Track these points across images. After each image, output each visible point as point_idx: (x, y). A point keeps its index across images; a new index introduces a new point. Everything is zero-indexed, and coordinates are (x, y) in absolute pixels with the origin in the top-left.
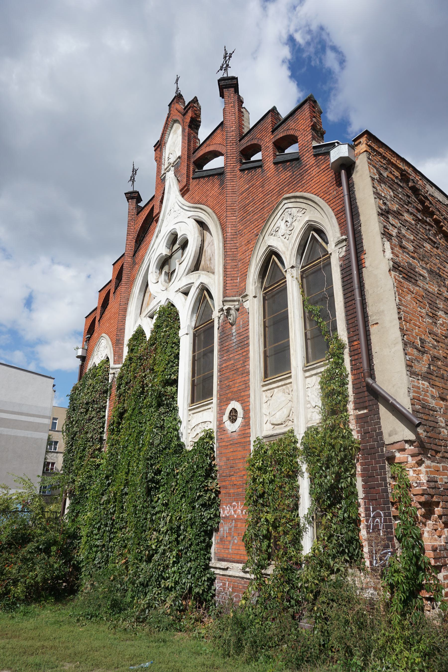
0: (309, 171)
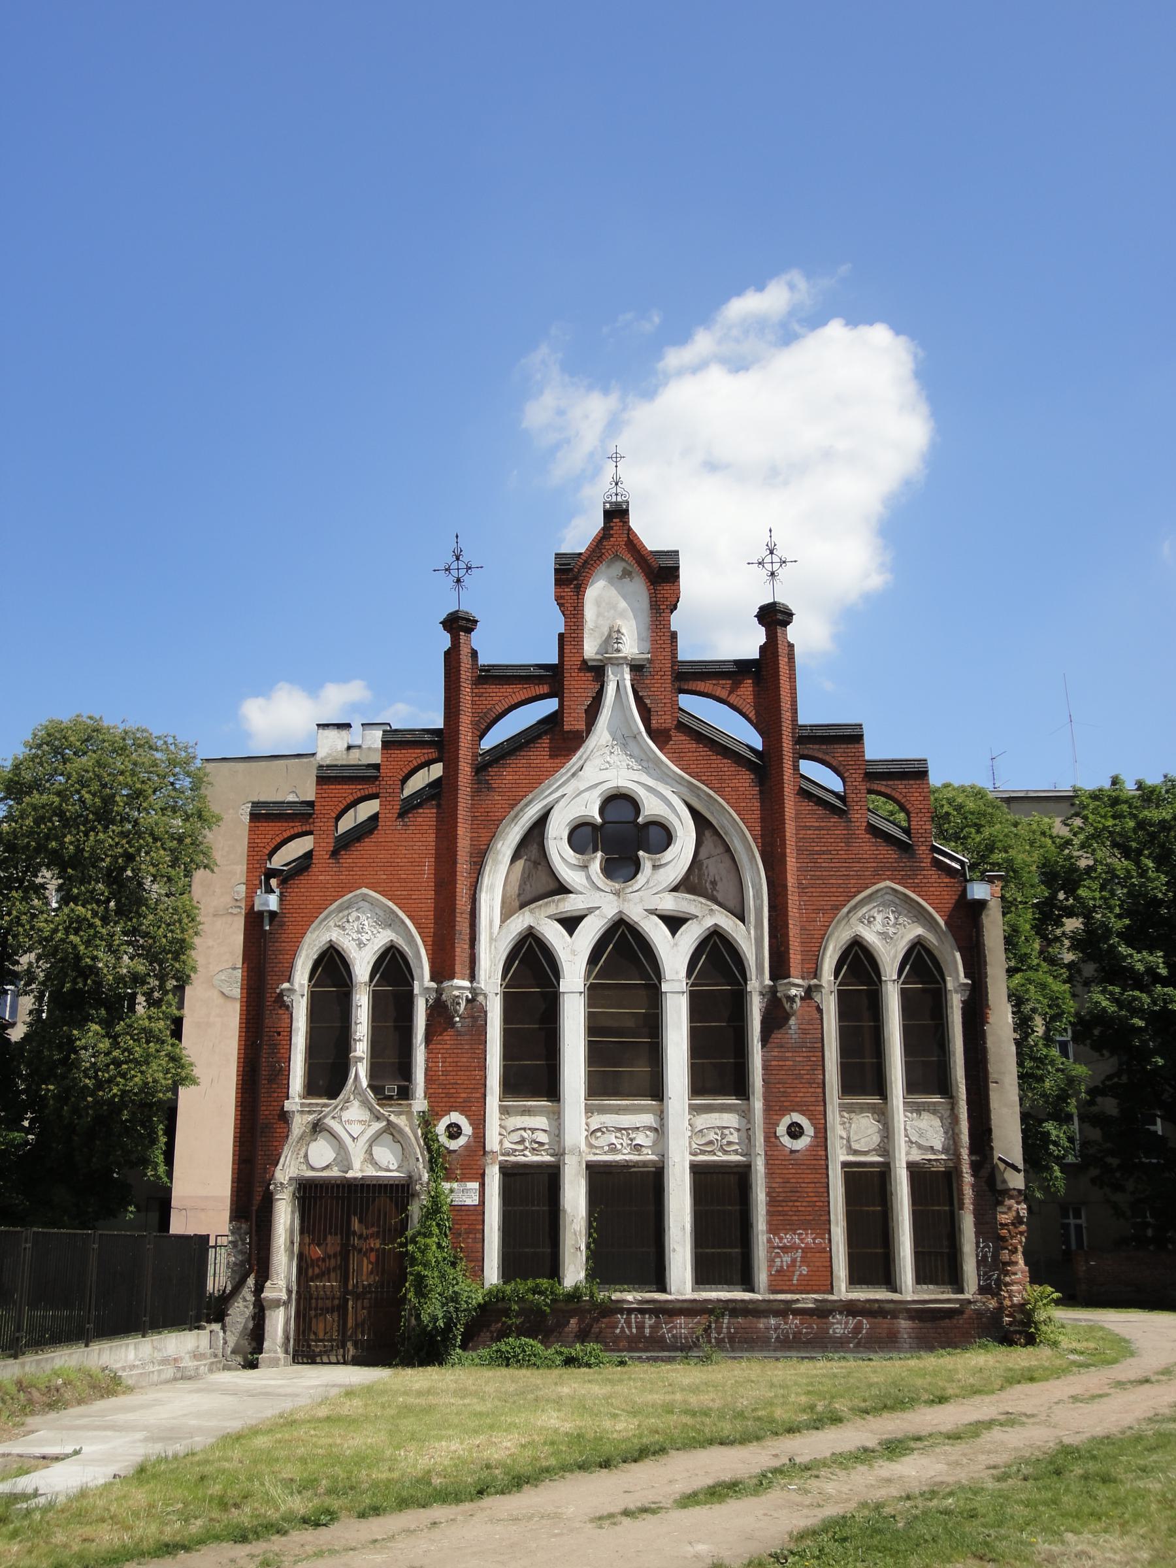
0: (925, 872)
